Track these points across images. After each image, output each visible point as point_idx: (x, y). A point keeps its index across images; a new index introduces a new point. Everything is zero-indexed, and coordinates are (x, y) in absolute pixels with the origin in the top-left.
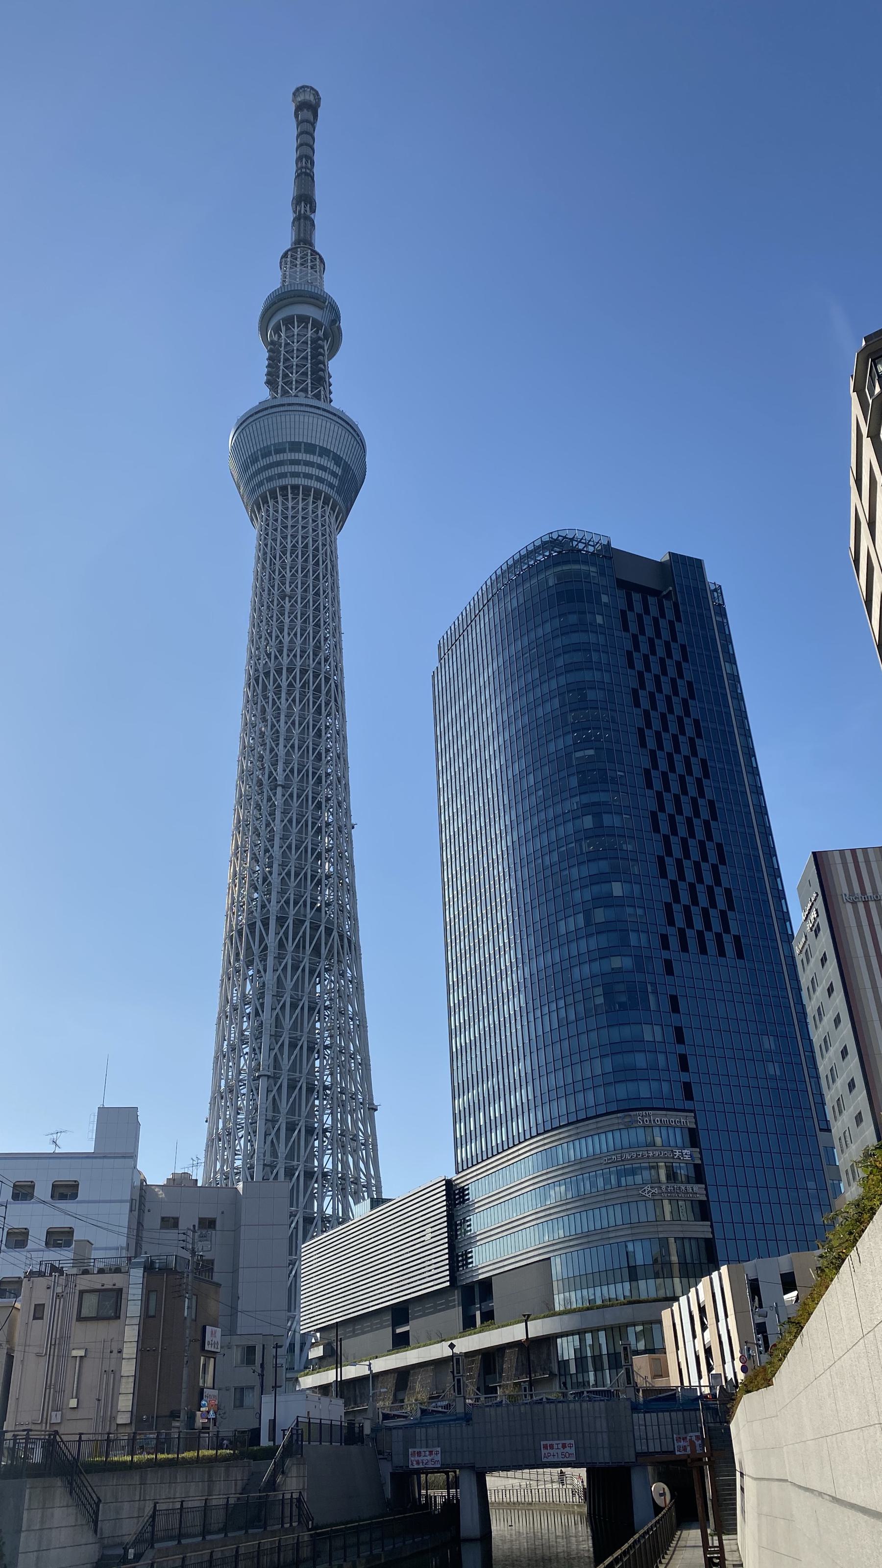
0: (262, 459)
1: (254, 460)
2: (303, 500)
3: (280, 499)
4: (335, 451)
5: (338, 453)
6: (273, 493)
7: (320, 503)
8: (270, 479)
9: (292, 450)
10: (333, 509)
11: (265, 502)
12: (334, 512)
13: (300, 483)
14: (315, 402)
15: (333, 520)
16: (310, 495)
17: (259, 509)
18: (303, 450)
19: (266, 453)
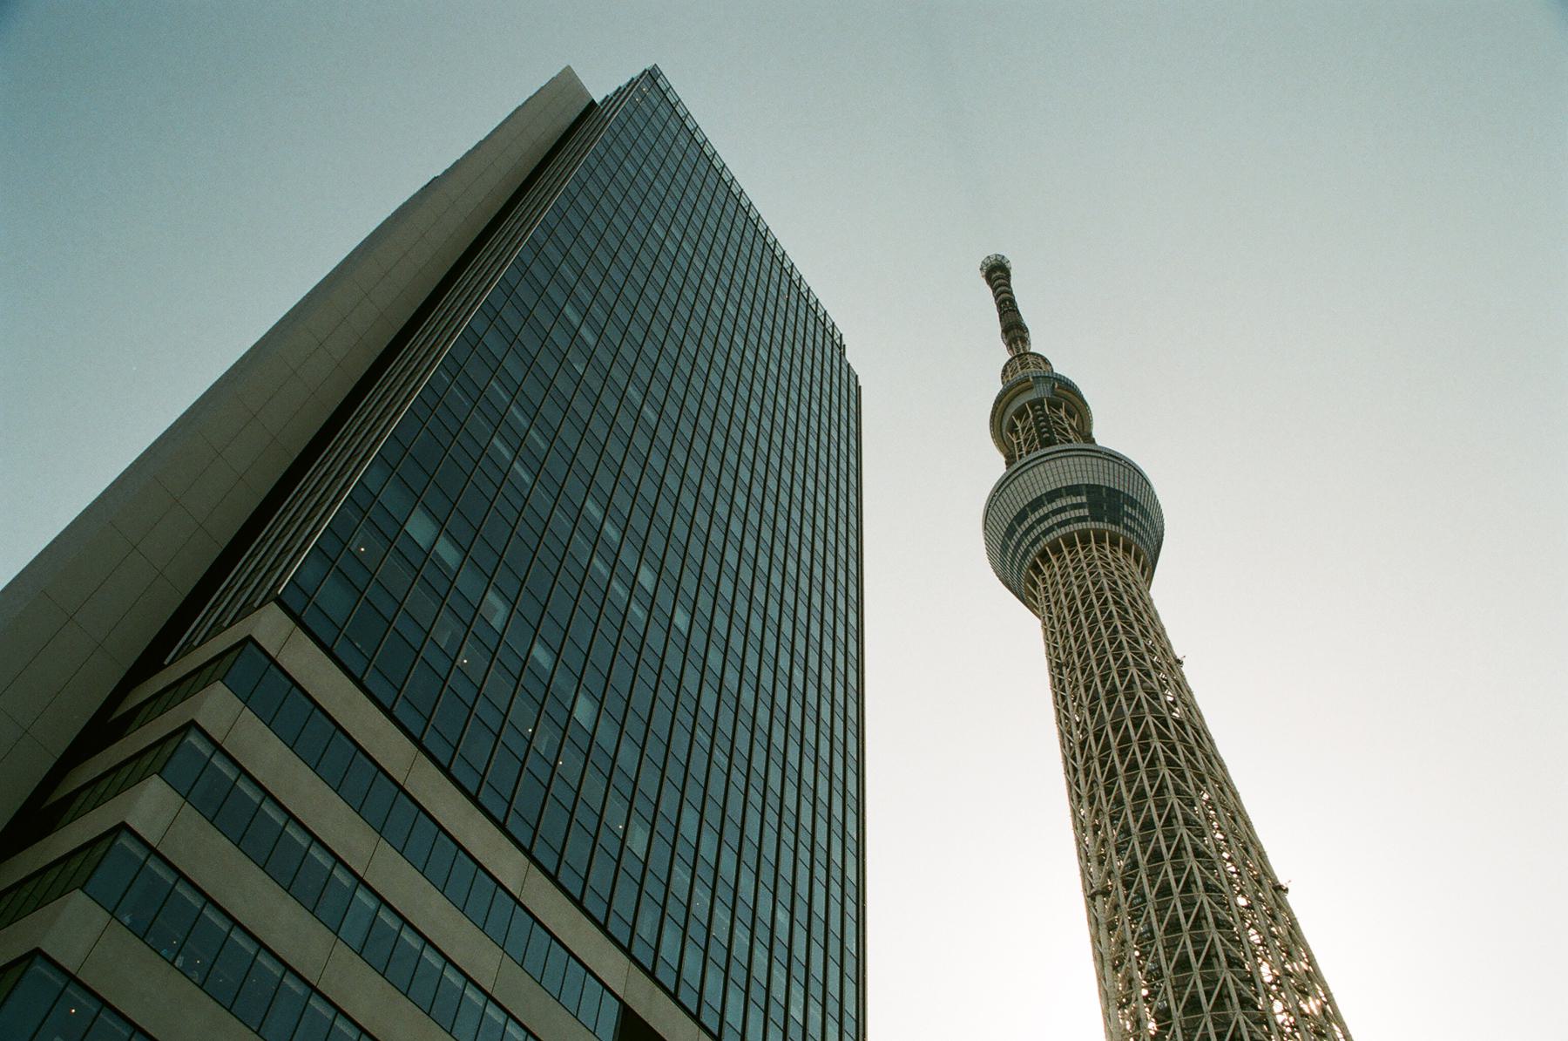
0: (1019, 526)
1: (1010, 532)
2: (1083, 549)
3: (1053, 559)
4: (1107, 485)
5: (1112, 486)
6: (1043, 556)
7: (1107, 546)
8: (1033, 544)
9: (1051, 501)
10: (1127, 549)
11: (1038, 571)
12: (1130, 554)
13: (1072, 530)
14: (1068, 446)
15: (1132, 562)
16: (1091, 541)
17: (1035, 585)
18: (1064, 494)
19: (1021, 517)
